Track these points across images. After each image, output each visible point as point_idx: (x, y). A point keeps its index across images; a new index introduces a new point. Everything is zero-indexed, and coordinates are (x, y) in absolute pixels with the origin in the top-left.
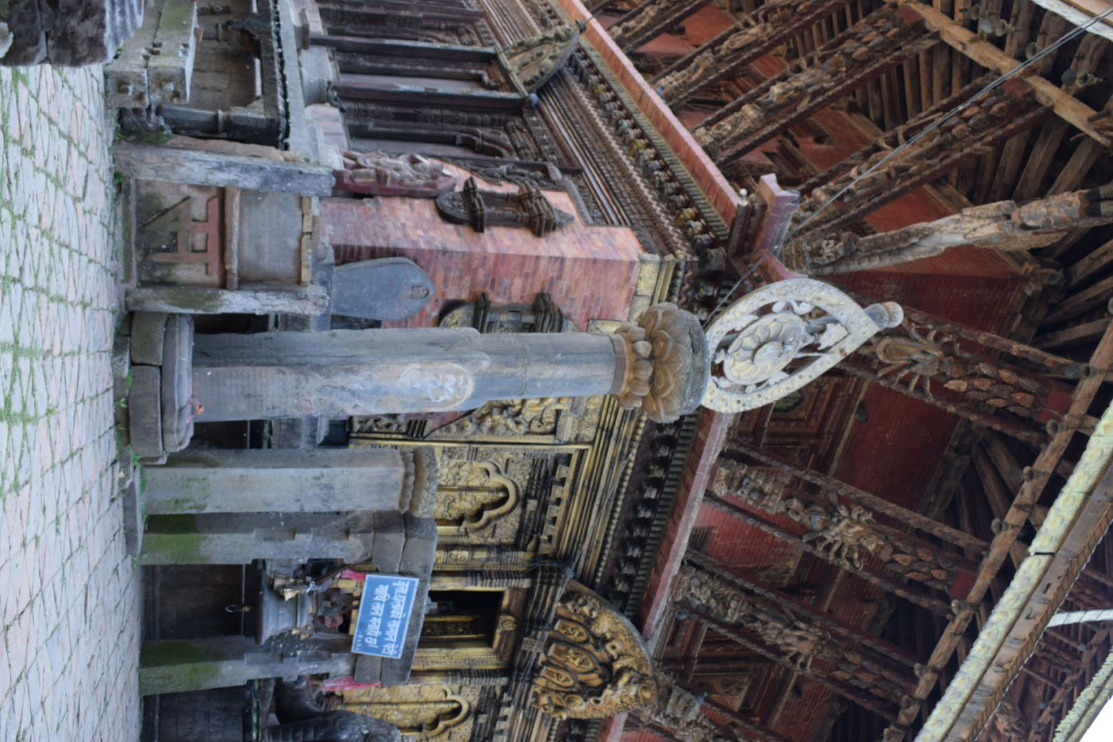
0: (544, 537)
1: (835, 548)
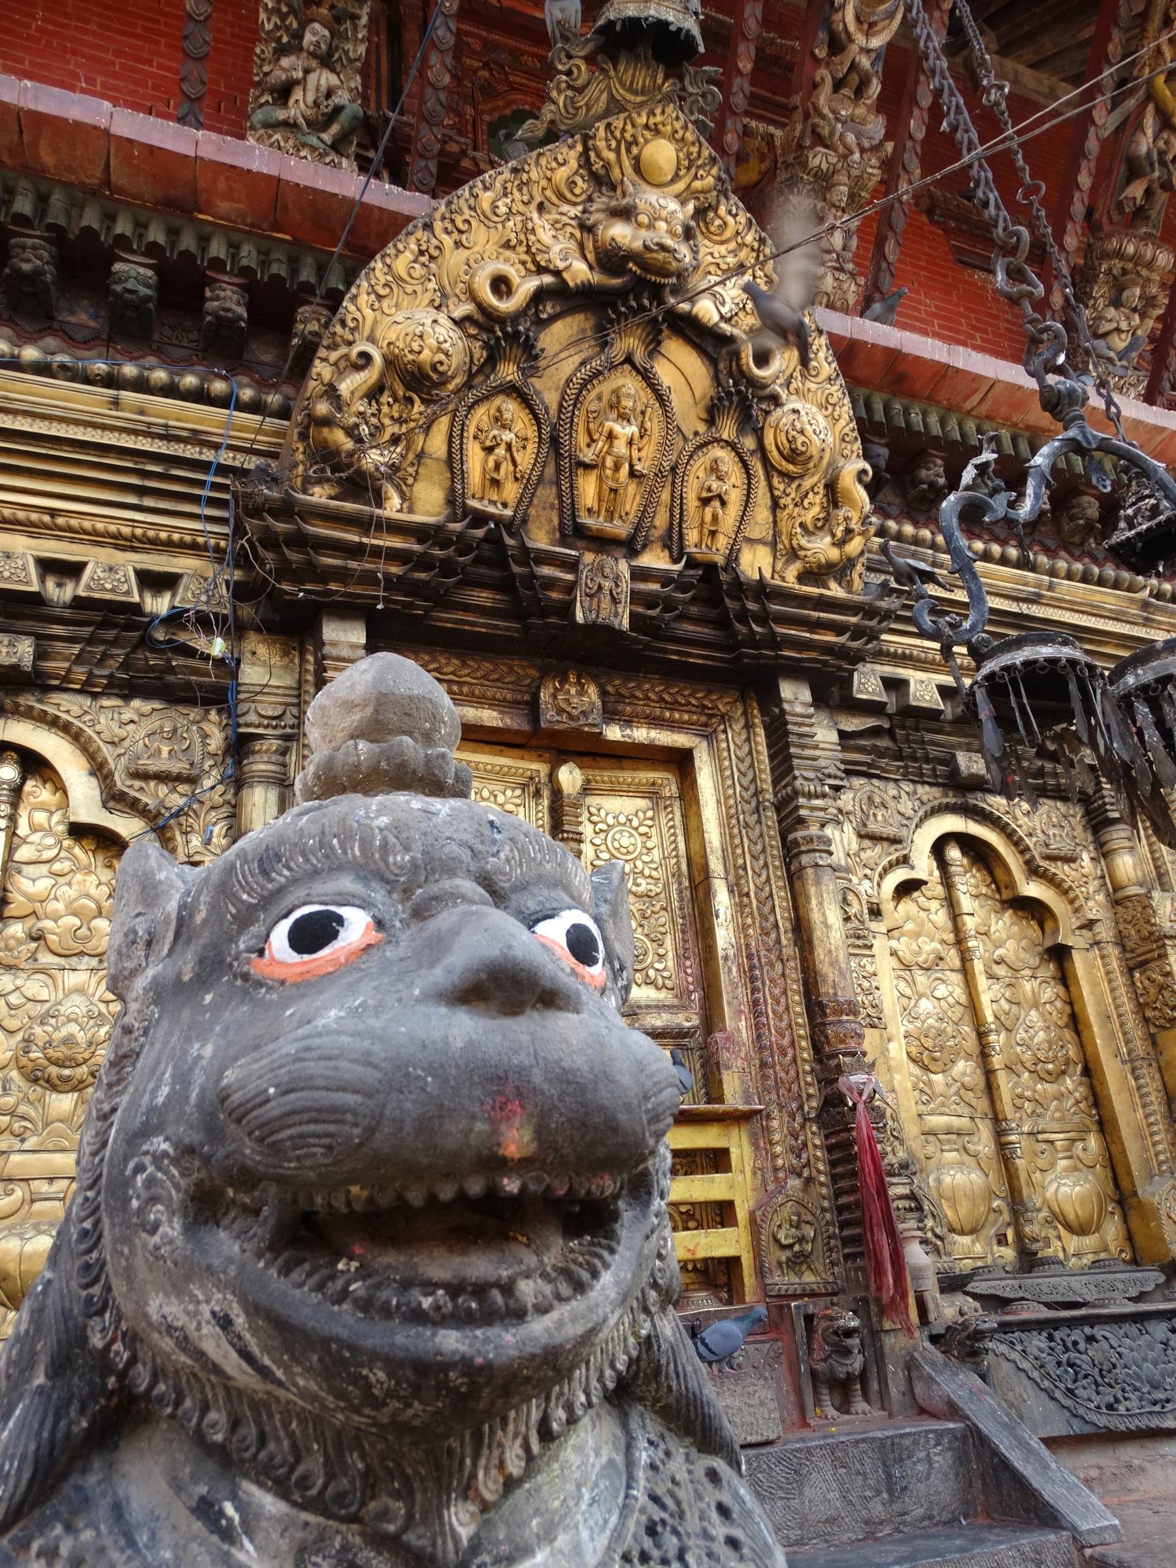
0: (159, 605)
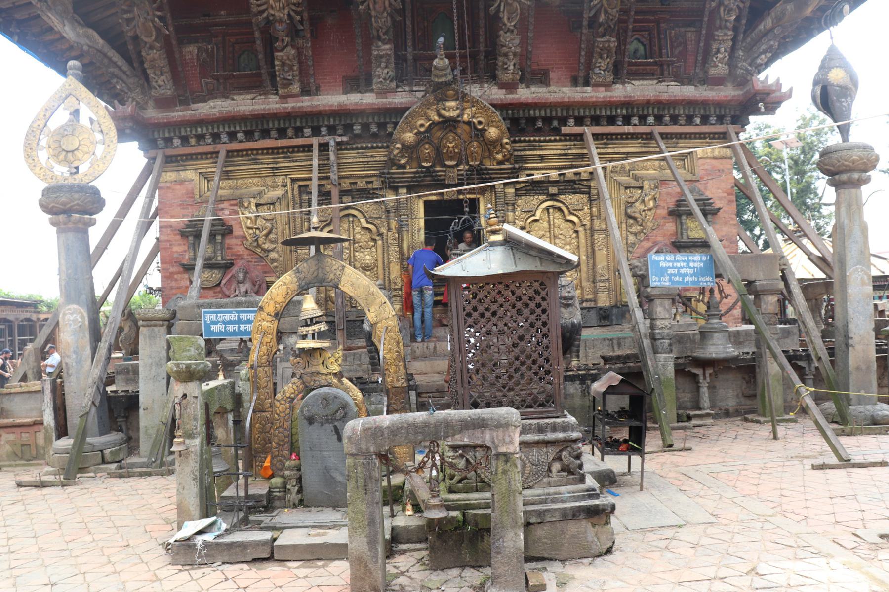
0: (370, 186)
1: (294, 8)
